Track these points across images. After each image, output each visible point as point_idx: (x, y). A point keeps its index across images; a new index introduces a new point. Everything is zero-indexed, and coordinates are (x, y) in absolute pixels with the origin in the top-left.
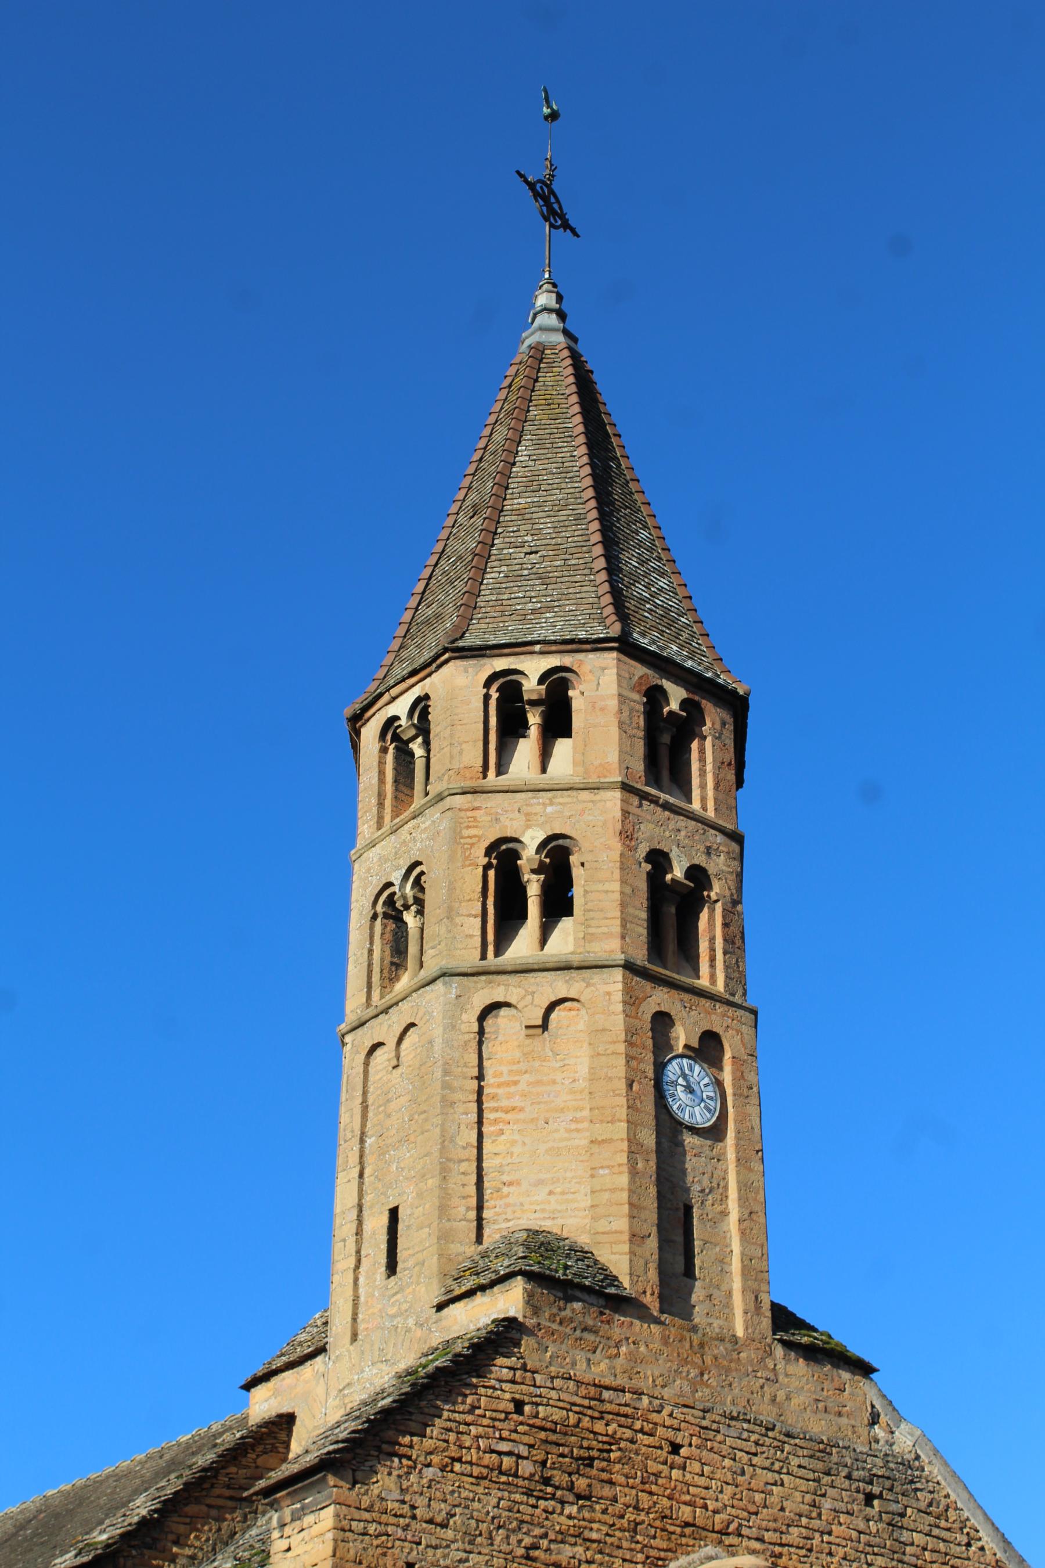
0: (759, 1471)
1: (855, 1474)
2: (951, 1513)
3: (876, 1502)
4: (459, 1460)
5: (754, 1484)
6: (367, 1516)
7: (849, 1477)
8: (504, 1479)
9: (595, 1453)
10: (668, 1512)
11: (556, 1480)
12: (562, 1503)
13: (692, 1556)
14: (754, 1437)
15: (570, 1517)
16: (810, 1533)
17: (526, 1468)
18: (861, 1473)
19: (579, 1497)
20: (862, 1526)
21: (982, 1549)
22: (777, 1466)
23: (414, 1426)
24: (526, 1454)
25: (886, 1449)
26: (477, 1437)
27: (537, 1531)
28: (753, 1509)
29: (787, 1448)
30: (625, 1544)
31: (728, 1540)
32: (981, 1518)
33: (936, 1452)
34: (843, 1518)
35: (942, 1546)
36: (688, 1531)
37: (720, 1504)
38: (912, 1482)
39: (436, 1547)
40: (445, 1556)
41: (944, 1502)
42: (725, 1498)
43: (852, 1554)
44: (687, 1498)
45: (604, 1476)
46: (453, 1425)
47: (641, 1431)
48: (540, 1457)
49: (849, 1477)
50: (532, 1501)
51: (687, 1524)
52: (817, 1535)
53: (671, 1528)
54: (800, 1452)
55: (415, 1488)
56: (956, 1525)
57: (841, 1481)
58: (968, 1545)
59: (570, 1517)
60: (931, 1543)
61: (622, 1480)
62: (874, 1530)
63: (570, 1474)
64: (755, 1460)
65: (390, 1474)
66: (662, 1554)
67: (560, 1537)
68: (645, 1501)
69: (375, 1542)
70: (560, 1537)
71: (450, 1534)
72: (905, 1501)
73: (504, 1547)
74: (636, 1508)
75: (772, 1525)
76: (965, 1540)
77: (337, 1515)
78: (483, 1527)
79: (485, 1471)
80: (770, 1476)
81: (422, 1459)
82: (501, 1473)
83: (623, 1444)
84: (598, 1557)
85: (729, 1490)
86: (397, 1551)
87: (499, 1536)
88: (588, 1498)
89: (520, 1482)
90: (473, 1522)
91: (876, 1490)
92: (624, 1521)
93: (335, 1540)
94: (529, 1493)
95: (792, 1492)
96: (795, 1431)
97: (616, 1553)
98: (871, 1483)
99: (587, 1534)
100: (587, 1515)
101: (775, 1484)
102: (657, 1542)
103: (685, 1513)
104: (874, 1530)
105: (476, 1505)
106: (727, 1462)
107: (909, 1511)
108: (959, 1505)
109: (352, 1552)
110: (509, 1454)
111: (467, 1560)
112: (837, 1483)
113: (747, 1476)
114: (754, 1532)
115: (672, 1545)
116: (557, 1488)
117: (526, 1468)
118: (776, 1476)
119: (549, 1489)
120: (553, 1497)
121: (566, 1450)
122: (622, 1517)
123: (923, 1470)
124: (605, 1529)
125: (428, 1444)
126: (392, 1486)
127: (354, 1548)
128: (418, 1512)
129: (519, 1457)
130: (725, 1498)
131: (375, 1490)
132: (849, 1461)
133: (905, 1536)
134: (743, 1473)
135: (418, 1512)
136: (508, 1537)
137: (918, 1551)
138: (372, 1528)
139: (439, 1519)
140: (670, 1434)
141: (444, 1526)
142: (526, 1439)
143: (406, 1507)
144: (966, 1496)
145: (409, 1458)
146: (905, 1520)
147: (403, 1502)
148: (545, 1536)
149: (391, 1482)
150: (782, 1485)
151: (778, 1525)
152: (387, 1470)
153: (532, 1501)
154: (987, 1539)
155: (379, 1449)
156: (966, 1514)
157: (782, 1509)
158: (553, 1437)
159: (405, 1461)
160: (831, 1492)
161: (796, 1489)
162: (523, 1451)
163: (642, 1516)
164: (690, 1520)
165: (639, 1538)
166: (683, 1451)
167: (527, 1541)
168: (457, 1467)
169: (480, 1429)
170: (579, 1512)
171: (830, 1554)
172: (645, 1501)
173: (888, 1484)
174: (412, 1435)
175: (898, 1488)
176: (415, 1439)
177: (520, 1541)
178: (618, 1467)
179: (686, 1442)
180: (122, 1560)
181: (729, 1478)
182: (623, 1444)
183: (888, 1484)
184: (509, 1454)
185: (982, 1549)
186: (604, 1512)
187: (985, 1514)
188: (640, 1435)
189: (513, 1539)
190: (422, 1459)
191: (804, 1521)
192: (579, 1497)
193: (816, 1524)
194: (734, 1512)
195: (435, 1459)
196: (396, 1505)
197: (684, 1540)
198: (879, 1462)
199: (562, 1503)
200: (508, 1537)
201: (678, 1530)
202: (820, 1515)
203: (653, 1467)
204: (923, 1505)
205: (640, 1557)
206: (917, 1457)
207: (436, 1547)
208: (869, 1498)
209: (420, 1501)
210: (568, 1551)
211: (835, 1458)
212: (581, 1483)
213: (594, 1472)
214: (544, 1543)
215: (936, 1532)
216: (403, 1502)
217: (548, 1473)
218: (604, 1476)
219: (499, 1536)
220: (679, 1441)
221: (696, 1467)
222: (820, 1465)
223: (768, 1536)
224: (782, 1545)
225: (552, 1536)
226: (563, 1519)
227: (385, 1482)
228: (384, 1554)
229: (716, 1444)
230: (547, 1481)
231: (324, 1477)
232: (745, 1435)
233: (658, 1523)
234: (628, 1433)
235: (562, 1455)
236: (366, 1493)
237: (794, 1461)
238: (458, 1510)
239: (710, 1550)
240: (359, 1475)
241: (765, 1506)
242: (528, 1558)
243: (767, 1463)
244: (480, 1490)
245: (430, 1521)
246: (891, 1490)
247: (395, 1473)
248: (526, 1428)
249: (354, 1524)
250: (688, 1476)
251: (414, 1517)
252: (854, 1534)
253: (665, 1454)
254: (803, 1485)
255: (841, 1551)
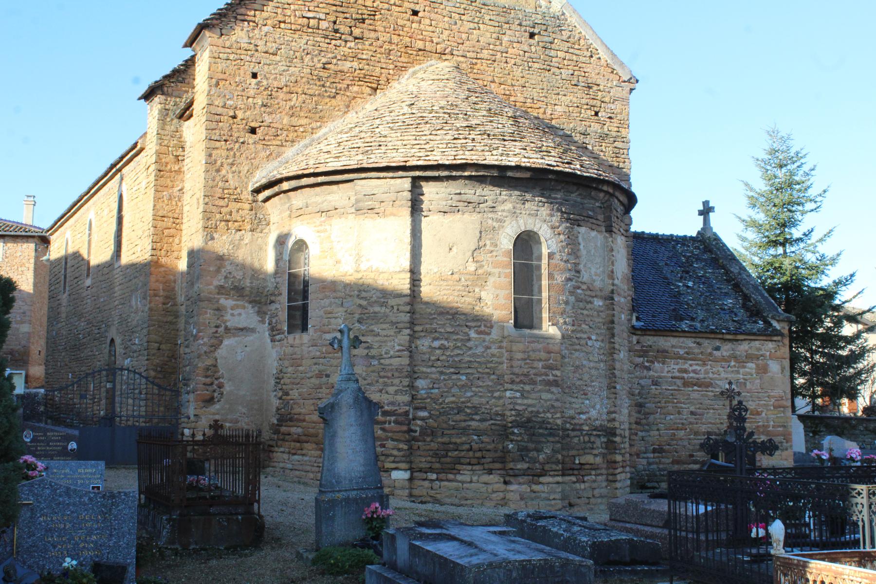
0: (465, 23)
1: (524, 23)
2: (582, 42)
3: (536, 37)
4: (284, 22)
5: (462, 29)
6: (229, 51)
7: (520, 25)
8: (310, 30)
9: (365, 17)
10: (409, 45)
11: (341, 31)
12: (346, 41)
13: (421, 66)
14: (463, 6)
15: (350, 48)
16: (495, 53)
17: (324, 25)
18: (528, 22)
19: (356, 38)
20: (526, 49)
21: (599, 58)
22: (476, 20)
23: (256, 6)
24: (323, 18)
25: (545, 10)
26: (295, 10)
27: (330, 55)
28: (461, 41)
29: (483, 11)
30: (382, 60)
31: (444, 57)
32: (599, 43)
33: (575, 11)
34: (515, 45)
35: (575, 58)
36: (420, 53)
37: (440, 40)
38: (559, 26)
39: (269, 65)
40: (274, 69)
41: (577, 36)
42: (444, 36)
43: (519, 62)
44: (421, 37)
45: (371, 27)
46: (280, 5)
47: (395, 4)
48: (333, 19)
49: (520, 25)
50: (328, 41)
51: (420, 50)
52: (499, 54)
53: (410, 52)
54: (491, 13)
55: (257, 36)
56: (585, 47)
57: (515, 27)
58: (592, 56)
59: (350, 48)
60: (568, 56)
61: (383, 29)
62: (534, 50)
63: (350, 27)
64: (463, 17)
65: (242, 30)
66: (405, 65)
67: (343, 58)
68: (395, 39)
69: (234, 63)
70: (343, 58)
71: (278, 58)
72: (554, 36)
73: (311, 64)
74: (390, 42)
75: (471, 49)
76: (589, 54)
77: (211, 51)
78: (297, 54)
79: (299, 27)
80: (472, 25)
81: (261, 22)
82: (308, 27)
83: (382, 12)
84: (366, 67)
85: (446, 33)
86: (246, 67)
87: (307, 59)
88: (362, 39)
89: (320, 32)
90: (292, 52)
91: (536, 31)
92: (383, 50)
93: (210, 63)
94: (326, 37)
95: (486, 34)
96: (488, 2)
97: (377, 64)
98: (534, 27)
99: (360, 56)
100: (360, 47)
101: (475, 29)
102: (403, 59)
103: (420, 45)
104: (534, 50)
105: (294, 44)
106: (446, 19)
107: (556, 41)
108: (587, 37)
109: (220, 68)
110: (314, 18)
111: (288, 70)
112: (513, 27)
113: (458, 25)
114: (461, 53)
115: (411, 60)
116: (343, 34)
117: (324, 25)
118: (476, 25)
119: (338, 35)
120: (340, 38)
121: (348, 15)
122: (381, 47)
123: (566, 20)
124: (371, 53)
125: (265, 14)
126: (244, 36)
127: (222, 65)
128: (259, 48)
129: (320, 19)
130: (444, 36)
131: (234, 38)
132: (521, 16)
133: (553, 53)
134: (456, 23)
135: (259, 48)
136: (312, 58)
137: (560, 60)
138: (232, 57)
139: (271, 51)
140: (412, 6)
141: (275, 54)
142: (324, 10)
143: (252, 47)
144: (591, 32)
145: (254, 22)
146: (553, 46)
147: (251, 43)
148: (336, 57)
149: (243, 34)
150: (479, 29)
151: (475, 49)
152: (240, 28)
153: (328, 41)
154: (602, 53)
155: (236, 18)
156: (591, 41)
157: (478, 41)
158: (340, 9)
159: (251, 24)
160: (508, 32)
161: (487, 31)
162: (323, 16)
163: (394, 47)
164: (422, 48)
165: (391, 57)
166: (420, 15)
167: (324, 60)
168: (282, 25)
169: (296, 6)
170: (356, 45)
171: (506, 62)
172: (395, 39)
173: (544, 27)
174: (255, 10)
175: (550, 29)
176: (257, 12)
177: (319, 61)
178: (379, 23)
179: (421, 9)
180: (166, 89)
181: (447, 26)
182: (382, 12)
183: (544, 27)
184: (314, 18)
185: (599, 58)
186: (371, 45)
187: (602, 41)
188: (394, 7)
189: (316, 60)
190: (261, 22)
191: (491, 47)
192: (356, 38)
193: (498, 48)
194: (449, 43)
195: (269, 22)
196: (246, 45)
197: (418, 58)
198: (539, 17)
199: (346, 41)
200: (312, 58)
201: (415, 53)
202: (501, 44)
203: (400, 22)
204: (564, 38)
205: (391, 66)
206: (563, 14)
207: (269, 65)
208: (532, 35)
209: (259, 43)
210: (348, 64)
211: (512, 15)
212: (357, 32)
213: (365, 26)
214: (334, 61)
215: (571, 50)
216: (251, 43)
217: (336, 27)
218: (371, 27)
219: (307, 59)
220: (417, 9)
221: (428, 22)
222: (503, 19)
223: (468, 55)
224: (477, 58)
225: (339, 57)
226: (346, 49)
227: (239, 34)
228: (239, 69)
229: (439, 11)
230: (336, 31)
231: (204, 34)
232: (458, 5)
233: (403, 50)
234: (386, 6)
235: (346, 18)
236: (228, 39)
237: (487, 17)
238: (283, 47)
239: (433, 62)
240: (224, 31)
241: (468, 40)
242: (324, 68)
243: (470, 19)
244: (296, 36)
245: (266, 52)
246: (546, 31)
247: (245, 29)
248: (324, 5)
249: (221, 55)
250: (422, 26)
251: (257, 51)
252: (522, 53)
253: (408, 15)
254: (492, 29)
255: (513, 61)
